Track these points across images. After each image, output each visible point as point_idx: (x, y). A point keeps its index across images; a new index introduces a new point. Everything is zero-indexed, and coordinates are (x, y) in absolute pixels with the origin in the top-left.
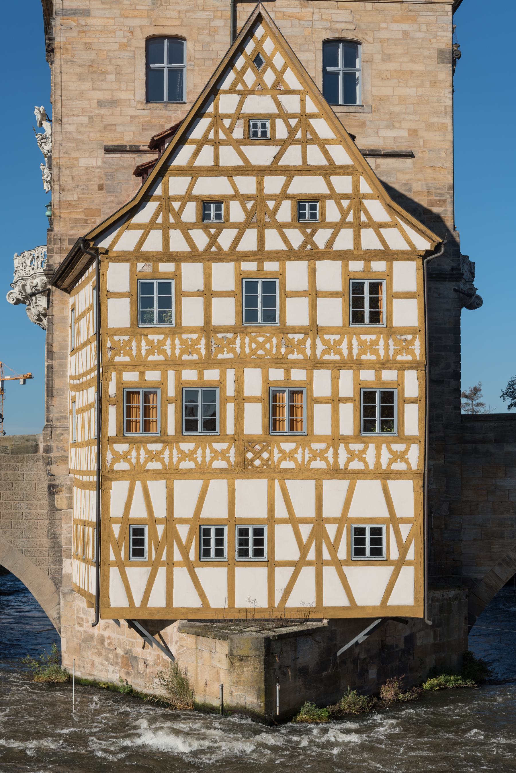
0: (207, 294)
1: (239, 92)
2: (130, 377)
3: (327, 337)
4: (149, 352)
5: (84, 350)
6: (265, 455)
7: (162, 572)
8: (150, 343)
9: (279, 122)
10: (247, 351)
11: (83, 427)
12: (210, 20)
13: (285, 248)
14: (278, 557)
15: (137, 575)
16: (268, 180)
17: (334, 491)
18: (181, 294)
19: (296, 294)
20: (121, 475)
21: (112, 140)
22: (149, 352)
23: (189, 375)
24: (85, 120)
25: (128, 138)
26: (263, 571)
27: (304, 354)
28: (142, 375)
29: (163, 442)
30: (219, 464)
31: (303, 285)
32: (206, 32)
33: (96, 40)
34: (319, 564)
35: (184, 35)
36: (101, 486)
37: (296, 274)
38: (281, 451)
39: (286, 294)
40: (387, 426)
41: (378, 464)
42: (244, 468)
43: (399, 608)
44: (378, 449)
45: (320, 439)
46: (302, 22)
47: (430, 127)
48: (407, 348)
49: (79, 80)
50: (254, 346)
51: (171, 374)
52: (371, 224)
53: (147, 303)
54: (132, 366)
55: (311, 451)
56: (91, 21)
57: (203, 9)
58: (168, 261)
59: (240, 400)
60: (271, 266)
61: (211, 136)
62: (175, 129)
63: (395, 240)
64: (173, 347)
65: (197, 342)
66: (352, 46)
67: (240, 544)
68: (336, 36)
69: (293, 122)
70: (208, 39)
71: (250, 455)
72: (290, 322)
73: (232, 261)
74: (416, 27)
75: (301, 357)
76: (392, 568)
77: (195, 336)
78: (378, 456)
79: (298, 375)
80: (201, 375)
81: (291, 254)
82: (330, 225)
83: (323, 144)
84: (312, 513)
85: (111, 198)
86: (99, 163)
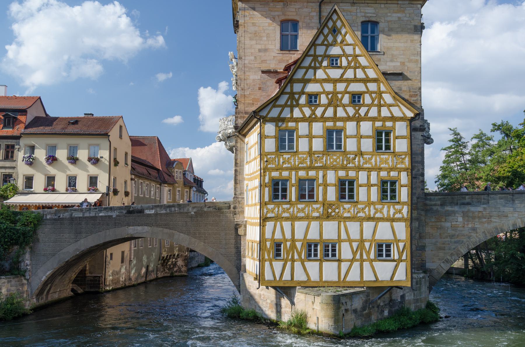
0: (310, 137)
1: (325, 45)
2: (275, 174)
3: (365, 156)
5: (253, 163)
6: (337, 211)
7: (289, 264)
9: (344, 59)
10: (329, 162)
11: (252, 197)
12: (310, 13)
13: (346, 116)
15: (278, 265)
17: (368, 226)
18: (299, 137)
19: (351, 137)
23: (302, 174)
24: (253, 58)
25: (272, 66)
26: (336, 264)
27: (354, 164)
28: (281, 173)
29: (290, 204)
30: (316, 214)
32: (308, 18)
33: (257, 22)
34: (362, 260)
37: (350, 127)
38: (344, 209)
39: (347, 137)
40: (393, 197)
44: (389, 208)
45: (363, 203)
46: (352, 13)
47: (410, 61)
49: (250, 40)
50: (332, 160)
54: (277, 170)
57: (307, 8)
59: (326, 185)
60: (339, 124)
61: (313, 65)
62: (295, 62)
63: (396, 112)
64: (295, 161)
66: (375, 24)
67: (325, 252)
68: (367, 19)
70: (309, 21)
71: (330, 211)
73: (322, 122)
74: (404, 15)
75: (353, 165)
77: (305, 156)
78: (388, 211)
81: (349, 119)
82: (367, 105)
83: (364, 68)
84: (358, 237)
85: (265, 94)
86: (259, 78)
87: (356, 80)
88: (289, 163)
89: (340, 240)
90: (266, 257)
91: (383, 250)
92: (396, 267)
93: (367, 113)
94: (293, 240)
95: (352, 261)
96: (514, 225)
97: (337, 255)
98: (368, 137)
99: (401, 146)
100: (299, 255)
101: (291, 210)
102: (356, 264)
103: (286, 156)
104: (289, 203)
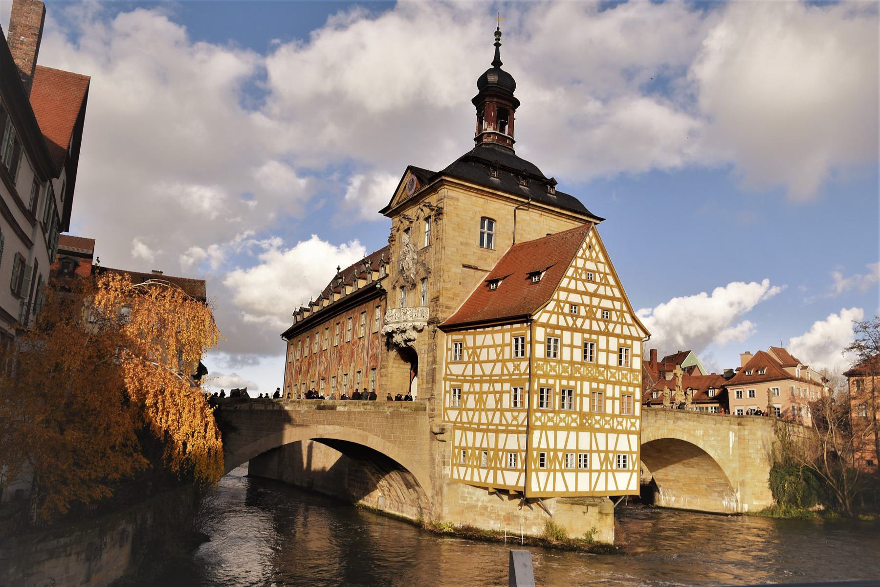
0: (572, 346)
2: (543, 381)
4: (550, 370)
7: (552, 474)
8: (551, 366)
9: (597, 274)
15: (543, 475)
18: (562, 345)
19: (602, 350)
20: (537, 428)
22: (550, 370)
30: (574, 425)
31: (604, 347)
34: (607, 471)
36: (527, 432)
39: (598, 350)
42: (581, 428)
45: (608, 415)
48: (636, 378)
51: (558, 381)
52: (626, 324)
53: (549, 347)
56: (459, 204)
59: (582, 395)
60: (594, 337)
64: (559, 369)
65: (567, 368)
72: (600, 363)
79: (602, 386)
81: (600, 333)
83: (611, 287)
84: (604, 448)
87: (606, 297)
88: (555, 371)
89: (591, 451)
91: (622, 461)
94: (556, 450)
95: (599, 471)
96: (648, 438)
97: (588, 465)
98: (613, 352)
99: (637, 364)
100: (560, 466)
102: (603, 474)
103: (553, 364)
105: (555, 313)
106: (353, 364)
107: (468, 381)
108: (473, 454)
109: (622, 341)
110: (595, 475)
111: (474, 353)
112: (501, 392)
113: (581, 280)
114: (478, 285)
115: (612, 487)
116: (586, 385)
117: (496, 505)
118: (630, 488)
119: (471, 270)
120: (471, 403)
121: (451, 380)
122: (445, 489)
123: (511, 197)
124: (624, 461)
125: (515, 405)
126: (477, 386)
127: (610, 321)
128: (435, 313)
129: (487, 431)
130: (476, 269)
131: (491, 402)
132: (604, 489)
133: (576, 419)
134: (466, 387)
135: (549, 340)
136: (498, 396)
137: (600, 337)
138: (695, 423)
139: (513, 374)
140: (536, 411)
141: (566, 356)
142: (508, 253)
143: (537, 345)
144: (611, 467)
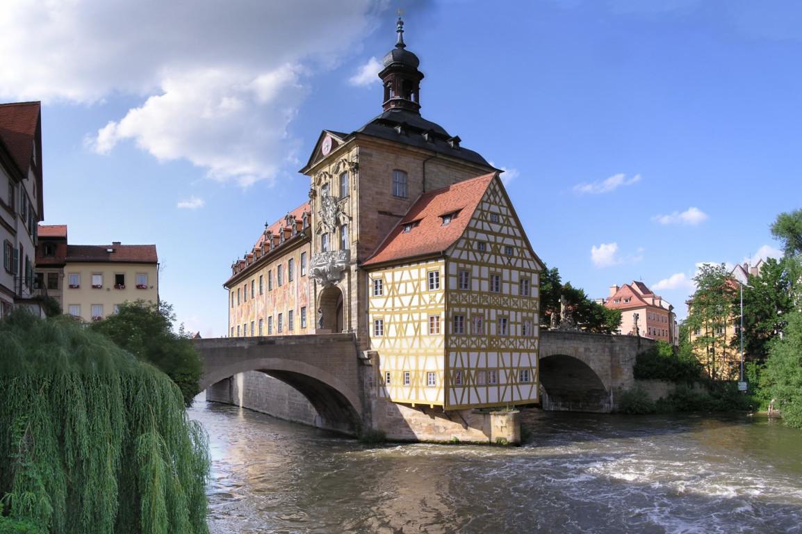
0: (480, 279)
2: (456, 310)
7: (467, 389)
9: (500, 217)
14: (501, 382)
15: (459, 391)
16: (498, 238)
20: (453, 350)
21: (381, 208)
23: (474, 310)
25: (387, 209)
26: (496, 388)
30: (483, 346)
31: (508, 279)
34: (512, 384)
35: (407, 171)
37: (506, 272)
41: (527, 347)
42: (490, 349)
43: (534, 400)
51: (468, 309)
55: (510, 342)
58: (469, 264)
60: (499, 270)
61: (481, 218)
65: (477, 297)
69: (505, 217)
71: (492, 343)
72: (504, 292)
76: (531, 386)
79: (506, 313)
80: (478, 311)
84: (509, 366)
87: (509, 236)
90: (450, 384)
92: (532, 387)
93: (515, 264)
94: (469, 369)
98: (515, 283)
99: (535, 293)
100: (474, 382)
101: (467, 342)
102: (509, 387)
104: (466, 335)
105: (466, 250)
106: (285, 305)
107: (389, 313)
108: (396, 377)
109: (522, 273)
110: (502, 388)
111: (393, 287)
112: (420, 322)
113: (487, 221)
114: (393, 229)
115: (517, 398)
116: (493, 312)
117: (418, 418)
118: (531, 398)
119: (387, 217)
120: (392, 332)
121: (373, 313)
122: (373, 407)
123: (421, 152)
124: (526, 376)
125: (432, 331)
126: (397, 317)
127: (512, 256)
128: (356, 255)
129: (407, 355)
130: (391, 214)
131: (410, 331)
132: (510, 400)
133: (485, 341)
134: (387, 319)
135: (461, 275)
136: (416, 324)
137: (504, 270)
138: (578, 342)
139: (430, 304)
140: (453, 335)
141: (475, 287)
142: (420, 199)
143: (451, 278)
144: (516, 381)
